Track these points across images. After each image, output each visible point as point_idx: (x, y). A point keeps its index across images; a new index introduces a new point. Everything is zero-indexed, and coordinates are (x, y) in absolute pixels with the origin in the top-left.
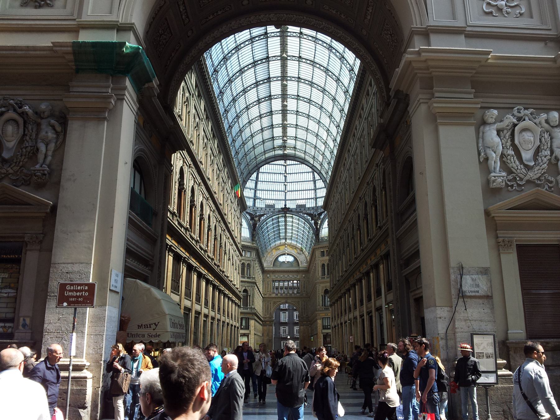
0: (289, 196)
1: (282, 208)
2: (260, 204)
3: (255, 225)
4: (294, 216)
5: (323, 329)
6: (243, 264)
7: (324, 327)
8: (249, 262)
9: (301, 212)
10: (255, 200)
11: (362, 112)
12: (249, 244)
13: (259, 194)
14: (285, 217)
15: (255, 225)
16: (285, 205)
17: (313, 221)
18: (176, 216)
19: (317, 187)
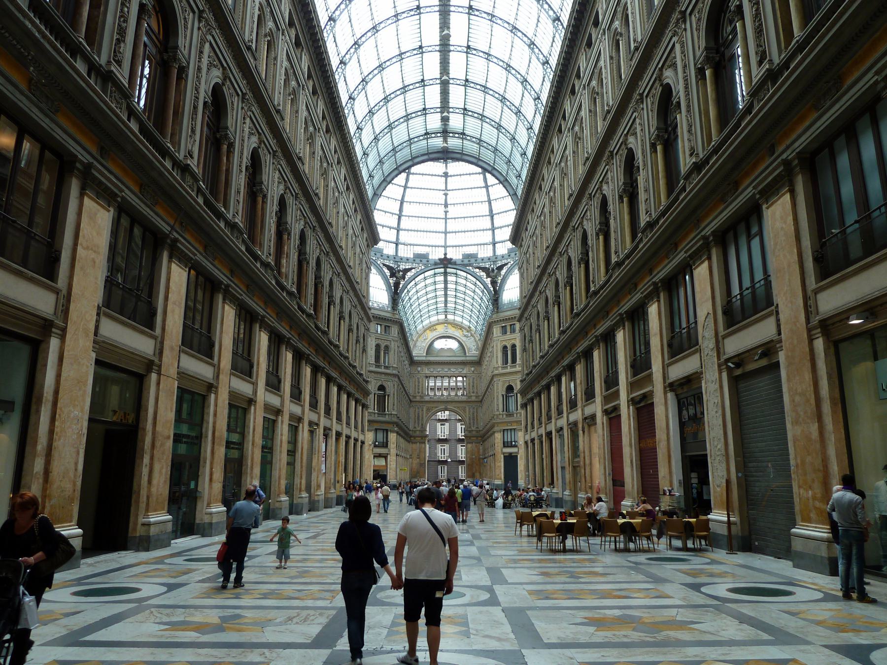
0: (452, 240)
1: (440, 259)
2: (405, 252)
3: (397, 285)
4: (459, 272)
5: (504, 446)
6: (378, 346)
7: (506, 445)
8: (388, 343)
9: (470, 265)
10: (397, 245)
11: (563, 122)
12: (388, 315)
13: (404, 237)
14: (445, 274)
15: (397, 285)
16: (445, 254)
17: (489, 279)
18: (273, 270)
19: (496, 225)
